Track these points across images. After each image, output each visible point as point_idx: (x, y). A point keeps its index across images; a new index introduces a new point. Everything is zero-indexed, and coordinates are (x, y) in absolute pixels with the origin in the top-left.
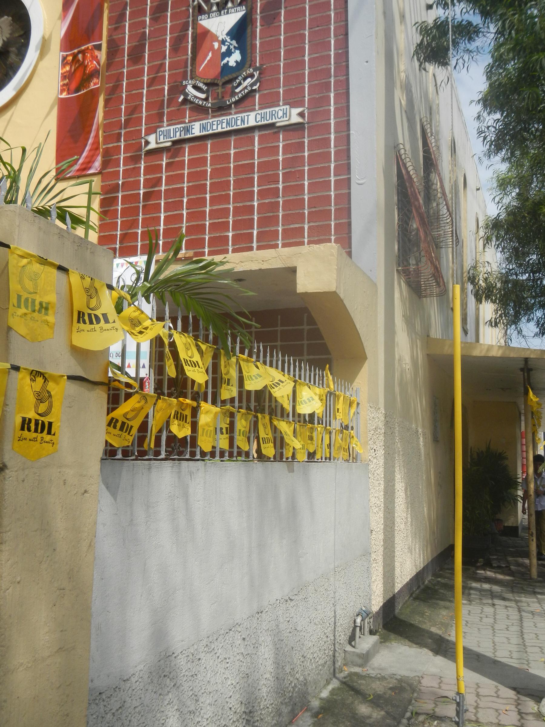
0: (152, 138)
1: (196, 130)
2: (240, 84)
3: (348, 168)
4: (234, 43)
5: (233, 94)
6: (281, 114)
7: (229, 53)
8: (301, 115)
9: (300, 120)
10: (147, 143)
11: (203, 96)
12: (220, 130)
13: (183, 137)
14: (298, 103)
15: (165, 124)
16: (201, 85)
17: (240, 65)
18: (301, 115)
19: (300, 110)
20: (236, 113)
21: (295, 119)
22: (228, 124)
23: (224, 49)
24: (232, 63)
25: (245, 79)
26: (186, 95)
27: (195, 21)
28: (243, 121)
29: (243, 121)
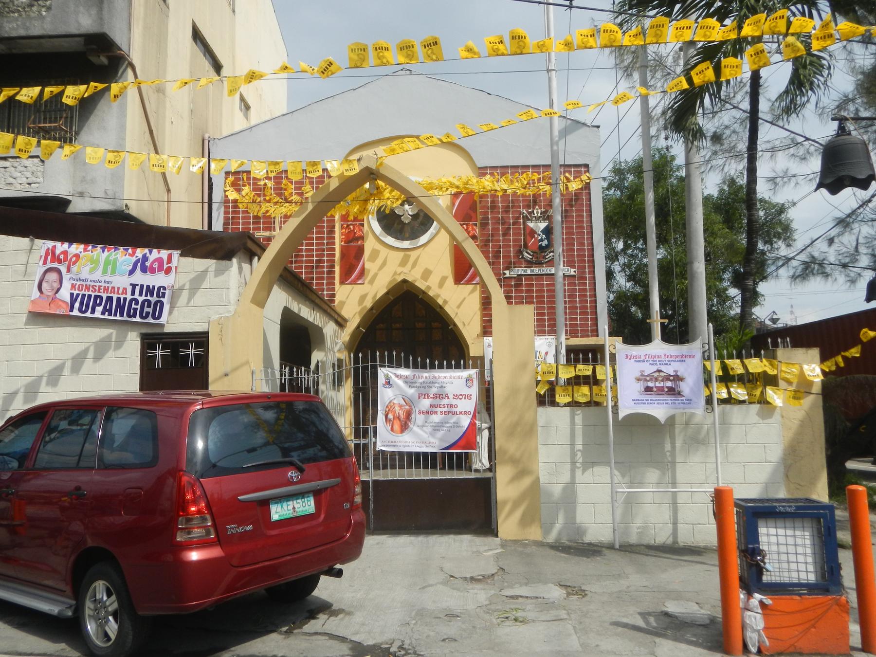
0: (507, 272)
1: (529, 272)
2: (548, 255)
3: (595, 296)
4: (544, 236)
5: (544, 257)
6: (566, 270)
7: (542, 240)
8: (575, 272)
9: (574, 274)
10: (504, 274)
11: (530, 257)
12: (539, 273)
13: (522, 273)
14: (573, 267)
15: (512, 266)
16: (530, 252)
17: (547, 246)
18: (575, 272)
19: (575, 270)
20: (546, 267)
21: (573, 273)
22: (543, 271)
23: (540, 238)
24: (543, 245)
25: (550, 253)
26: (523, 255)
27: (524, 223)
28: (550, 270)
29: (550, 270)
